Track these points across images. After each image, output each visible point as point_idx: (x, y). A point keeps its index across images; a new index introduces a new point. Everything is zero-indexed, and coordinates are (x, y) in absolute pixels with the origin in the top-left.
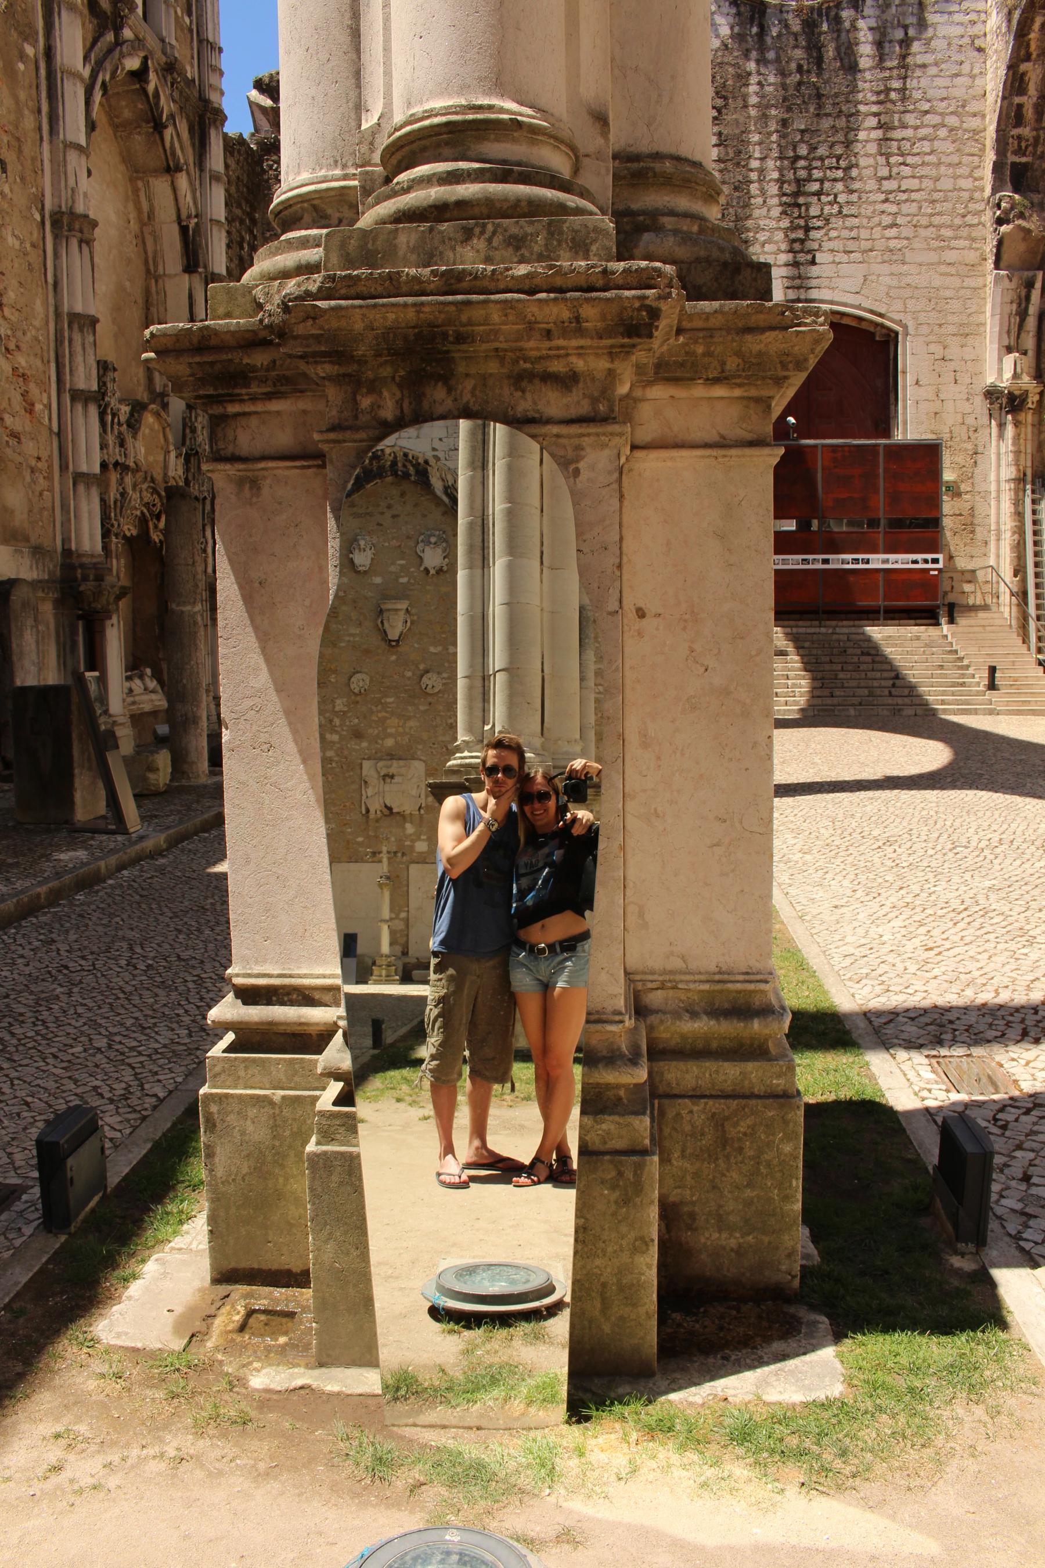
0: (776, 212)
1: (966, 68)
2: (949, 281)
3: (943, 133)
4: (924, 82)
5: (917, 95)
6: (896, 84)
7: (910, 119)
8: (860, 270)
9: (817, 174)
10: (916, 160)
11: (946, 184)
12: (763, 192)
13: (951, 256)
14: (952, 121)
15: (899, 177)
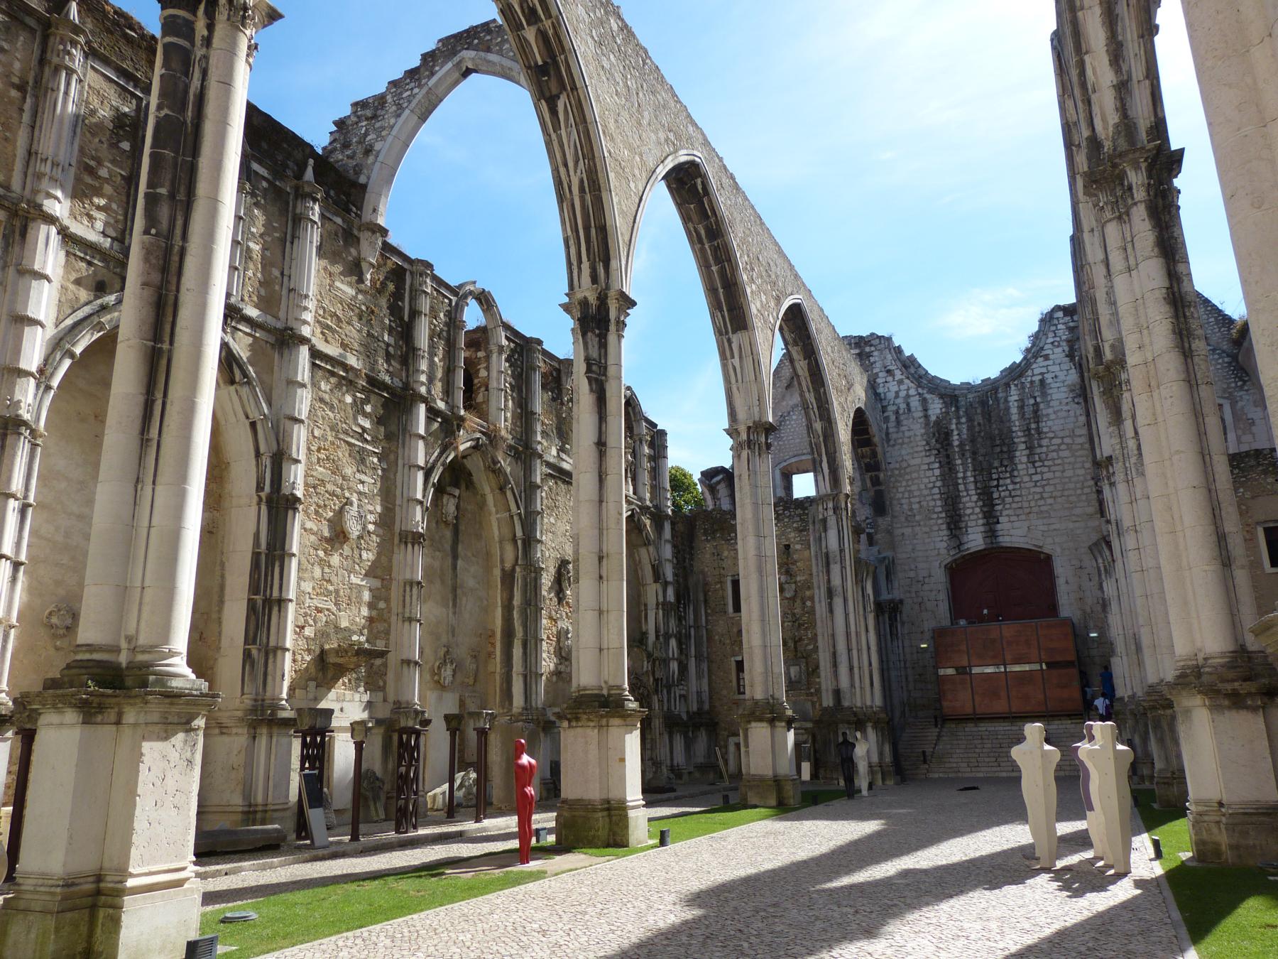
0: (975, 498)
1: (1072, 413)
2: (1077, 525)
3: (1063, 447)
4: (1049, 423)
5: (1045, 430)
6: (1033, 426)
7: (1045, 442)
8: (1027, 524)
9: (995, 476)
10: (1050, 463)
11: (1069, 473)
12: (967, 490)
13: (1078, 511)
14: (1067, 440)
15: (1042, 473)
